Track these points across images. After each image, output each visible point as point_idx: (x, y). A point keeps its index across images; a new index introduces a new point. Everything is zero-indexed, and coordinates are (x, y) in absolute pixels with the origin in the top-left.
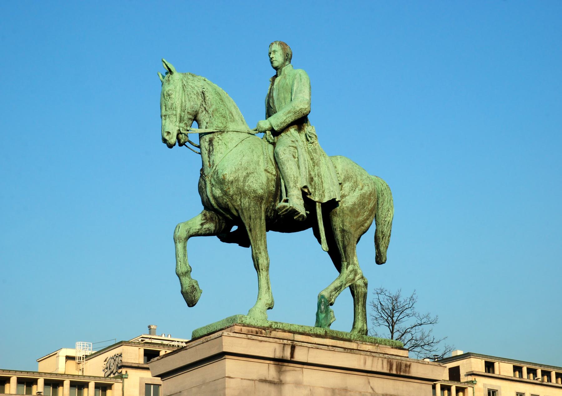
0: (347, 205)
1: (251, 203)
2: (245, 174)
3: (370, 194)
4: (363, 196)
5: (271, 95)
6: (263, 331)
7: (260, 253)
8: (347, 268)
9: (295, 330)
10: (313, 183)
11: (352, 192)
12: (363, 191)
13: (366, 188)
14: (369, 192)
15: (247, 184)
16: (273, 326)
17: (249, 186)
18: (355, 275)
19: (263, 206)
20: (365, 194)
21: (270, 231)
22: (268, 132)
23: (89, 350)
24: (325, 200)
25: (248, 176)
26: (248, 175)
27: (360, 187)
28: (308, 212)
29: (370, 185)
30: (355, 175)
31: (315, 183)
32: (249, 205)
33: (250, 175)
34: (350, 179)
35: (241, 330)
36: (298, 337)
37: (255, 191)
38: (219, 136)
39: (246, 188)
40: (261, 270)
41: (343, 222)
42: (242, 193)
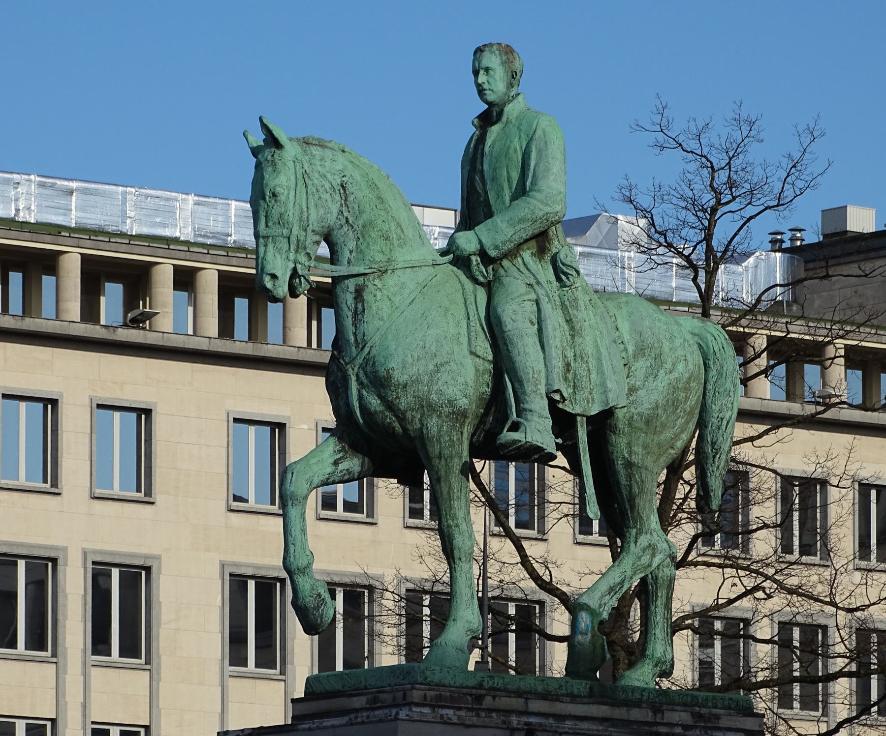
0: (639, 410)
2: (431, 367)
7: (457, 526)
10: (570, 376)
11: (651, 379)
12: (675, 375)
13: (681, 367)
15: (436, 388)
16: (485, 684)
17: (440, 392)
20: (677, 380)
25: (438, 371)
27: (669, 366)
31: (575, 375)
32: (439, 431)
34: (647, 352)
37: (451, 403)
39: (434, 397)
41: (629, 445)
42: (427, 407)
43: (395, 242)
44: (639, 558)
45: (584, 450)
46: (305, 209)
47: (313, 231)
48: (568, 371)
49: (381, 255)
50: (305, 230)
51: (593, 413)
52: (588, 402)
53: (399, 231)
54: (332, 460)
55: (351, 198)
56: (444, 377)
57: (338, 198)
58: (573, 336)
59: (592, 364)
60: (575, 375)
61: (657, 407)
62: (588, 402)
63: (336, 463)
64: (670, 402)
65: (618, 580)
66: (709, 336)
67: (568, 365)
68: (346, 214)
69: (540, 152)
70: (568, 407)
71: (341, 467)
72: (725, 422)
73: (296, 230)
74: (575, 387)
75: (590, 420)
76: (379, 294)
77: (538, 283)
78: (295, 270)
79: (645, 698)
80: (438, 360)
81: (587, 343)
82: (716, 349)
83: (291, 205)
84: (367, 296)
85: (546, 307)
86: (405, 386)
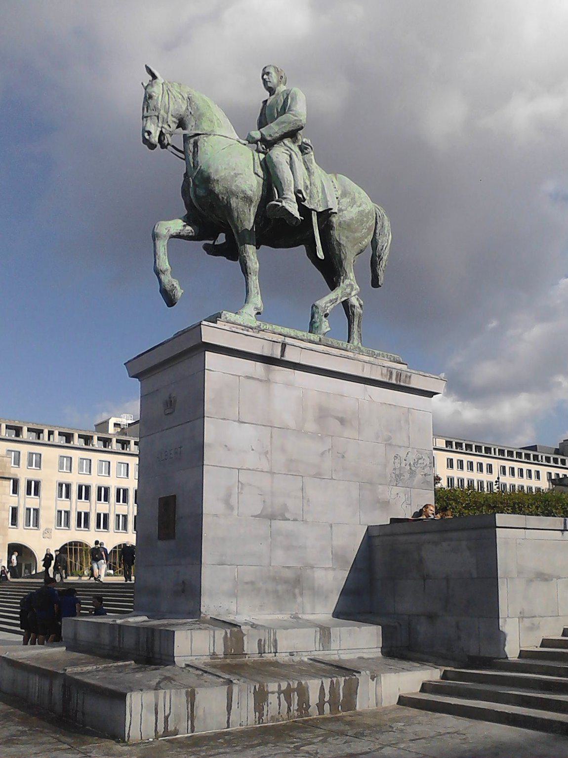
0: (344, 219)
1: (238, 203)
3: (369, 212)
4: (360, 213)
5: (264, 112)
6: (250, 330)
8: (343, 282)
9: (286, 334)
12: (361, 209)
18: (352, 290)
19: (252, 209)
20: (363, 211)
21: (262, 246)
22: (259, 143)
23: (131, 420)
24: (321, 210)
26: (236, 175)
27: (359, 204)
28: (302, 218)
30: (353, 192)
32: (237, 206)
36: (288, 340)
37: (243, 192)
38: (205, 138)
40: (249, 275)
42: (231, 193)
45: (315, 226)
46: (167, 104)
47: (172, 115)
51: (320, 211)
52: (317, 205)
58: (309, 176)
59: (320, 190)
61: (352, 219)
62: (317, 205)
67: (307, 187)
68: (190, 110)
69: (292, 99)
72: (384, 247)
73: (162, 112)
76: (206, 144)
78: (161, 131)
85: (294, 156)
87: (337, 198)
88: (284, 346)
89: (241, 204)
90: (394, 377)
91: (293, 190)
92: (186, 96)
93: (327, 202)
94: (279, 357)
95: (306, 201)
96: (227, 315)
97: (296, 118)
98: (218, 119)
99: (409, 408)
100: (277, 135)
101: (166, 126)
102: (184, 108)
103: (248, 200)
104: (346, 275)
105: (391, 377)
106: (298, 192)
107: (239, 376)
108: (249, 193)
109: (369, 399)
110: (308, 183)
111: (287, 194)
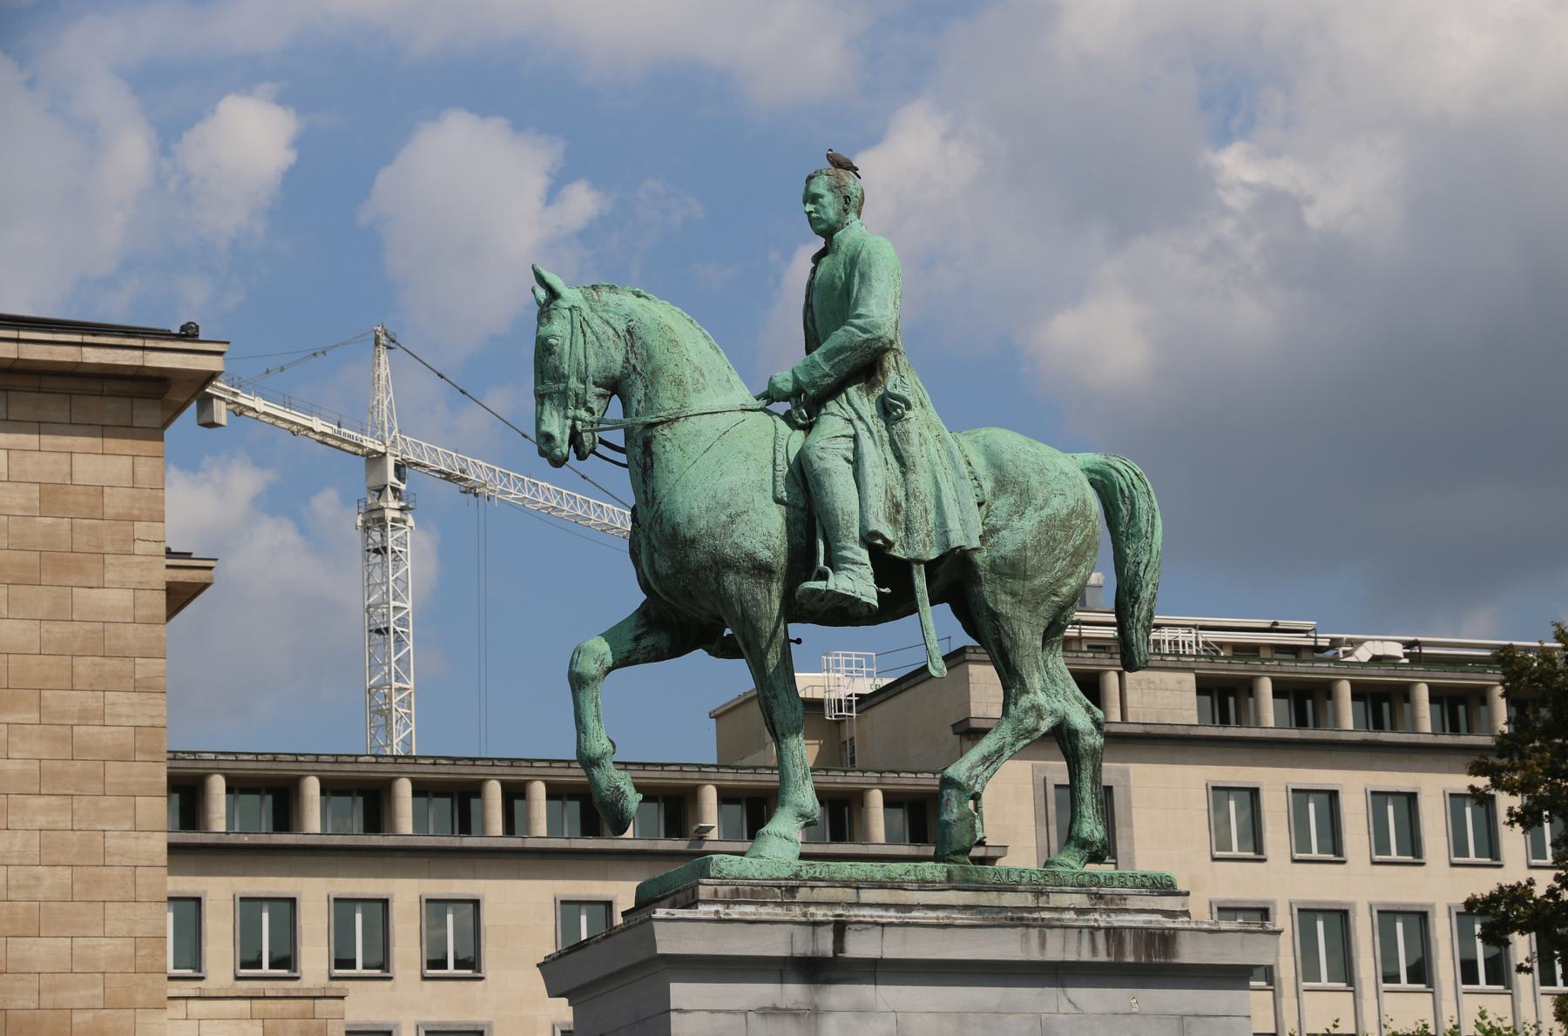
0: (1002, 552)
2: (723, 518)
4: (1048, 525)
7: (775, 697)
10: (901, 518)
11: (1016, 517)
12: (1048, 511)
13: (1056, 502)
14: (1065, 511)
16: (803, 874)
17: (737, 546)
20: (1051, 518)
24: (933, 554)
26: (732, 519)
27: (1040, 502)
29: (1067, 491)
31: (907, 517)
33: (738, 520)
34: (1010, 488)
35: (716, 892)
37: (751, 557)
39: (728, 551)
41: (993, 592)
42: (722, 564)
43: (690, 387)
44: (1021, 721)
48: (898, 512)
49: (671, 403)
50: (584, 382)
52: (925, 545)
53: (697, 375)
54: (631, 636)
55: (638, 343)
56: (740, 528)
57: (622, 344)
58: (904, 474)
59: (930, 503)
60: (907, 517)
61: (1025, 548)
63: (637, 639)
64: (1043, 543)
65: (993, 748)
66: (1114, 473)
67: (897, 506)
68: (633, 361)
69: (862, 276)
70: (898, 552)
71: (643, 643)
72: (1142, 567)
73: (574, 383)
74: (907, 529)
75: (931, 567)
76: (668, 445)
77: (860, 418)
78: (573, 427)
79: (1025, 880)
80: (732, 510)
81: (921, 480)
82: (1124, 485)
83: (566, 357)
84: (656, 448)
85: (866, 443)
86: (693, 541)
87: (980, 505)
88: (840, 928)
89: (747, 584)
90: (1129, 947)
91: (857, 535)
92: (622, 327)
93: (945, 533)
94: (830, 954)
95: (897, 546)
96: (723, 865)
97: (866, 336)
98: (696, 368)
99: (1183, 1016)
100: (829, 381)
101: (583, 413)
102: (619, 358)
103: (762, 570)
104: (1023, 683)
105: (1120, 951)
106: (869, 540)
107: (745, 1013)
108: (765, 555)
109: (1071, 1009)
110: (900, 494)
111: (845, 548)
